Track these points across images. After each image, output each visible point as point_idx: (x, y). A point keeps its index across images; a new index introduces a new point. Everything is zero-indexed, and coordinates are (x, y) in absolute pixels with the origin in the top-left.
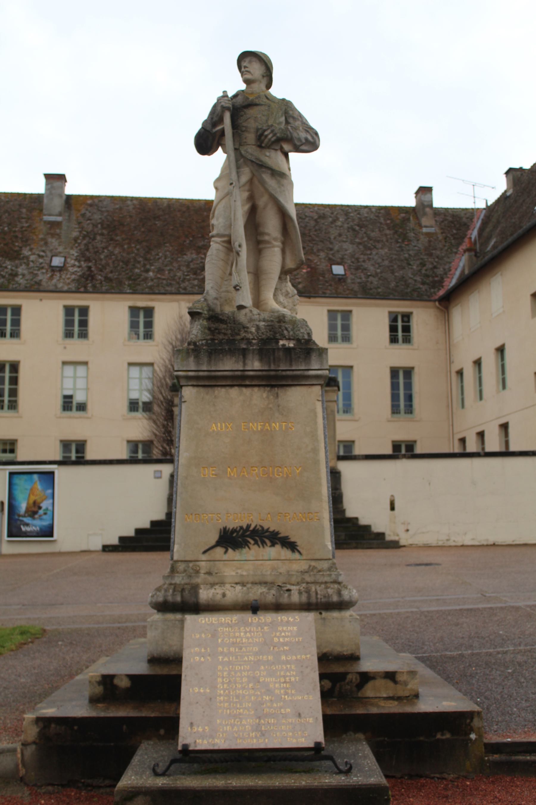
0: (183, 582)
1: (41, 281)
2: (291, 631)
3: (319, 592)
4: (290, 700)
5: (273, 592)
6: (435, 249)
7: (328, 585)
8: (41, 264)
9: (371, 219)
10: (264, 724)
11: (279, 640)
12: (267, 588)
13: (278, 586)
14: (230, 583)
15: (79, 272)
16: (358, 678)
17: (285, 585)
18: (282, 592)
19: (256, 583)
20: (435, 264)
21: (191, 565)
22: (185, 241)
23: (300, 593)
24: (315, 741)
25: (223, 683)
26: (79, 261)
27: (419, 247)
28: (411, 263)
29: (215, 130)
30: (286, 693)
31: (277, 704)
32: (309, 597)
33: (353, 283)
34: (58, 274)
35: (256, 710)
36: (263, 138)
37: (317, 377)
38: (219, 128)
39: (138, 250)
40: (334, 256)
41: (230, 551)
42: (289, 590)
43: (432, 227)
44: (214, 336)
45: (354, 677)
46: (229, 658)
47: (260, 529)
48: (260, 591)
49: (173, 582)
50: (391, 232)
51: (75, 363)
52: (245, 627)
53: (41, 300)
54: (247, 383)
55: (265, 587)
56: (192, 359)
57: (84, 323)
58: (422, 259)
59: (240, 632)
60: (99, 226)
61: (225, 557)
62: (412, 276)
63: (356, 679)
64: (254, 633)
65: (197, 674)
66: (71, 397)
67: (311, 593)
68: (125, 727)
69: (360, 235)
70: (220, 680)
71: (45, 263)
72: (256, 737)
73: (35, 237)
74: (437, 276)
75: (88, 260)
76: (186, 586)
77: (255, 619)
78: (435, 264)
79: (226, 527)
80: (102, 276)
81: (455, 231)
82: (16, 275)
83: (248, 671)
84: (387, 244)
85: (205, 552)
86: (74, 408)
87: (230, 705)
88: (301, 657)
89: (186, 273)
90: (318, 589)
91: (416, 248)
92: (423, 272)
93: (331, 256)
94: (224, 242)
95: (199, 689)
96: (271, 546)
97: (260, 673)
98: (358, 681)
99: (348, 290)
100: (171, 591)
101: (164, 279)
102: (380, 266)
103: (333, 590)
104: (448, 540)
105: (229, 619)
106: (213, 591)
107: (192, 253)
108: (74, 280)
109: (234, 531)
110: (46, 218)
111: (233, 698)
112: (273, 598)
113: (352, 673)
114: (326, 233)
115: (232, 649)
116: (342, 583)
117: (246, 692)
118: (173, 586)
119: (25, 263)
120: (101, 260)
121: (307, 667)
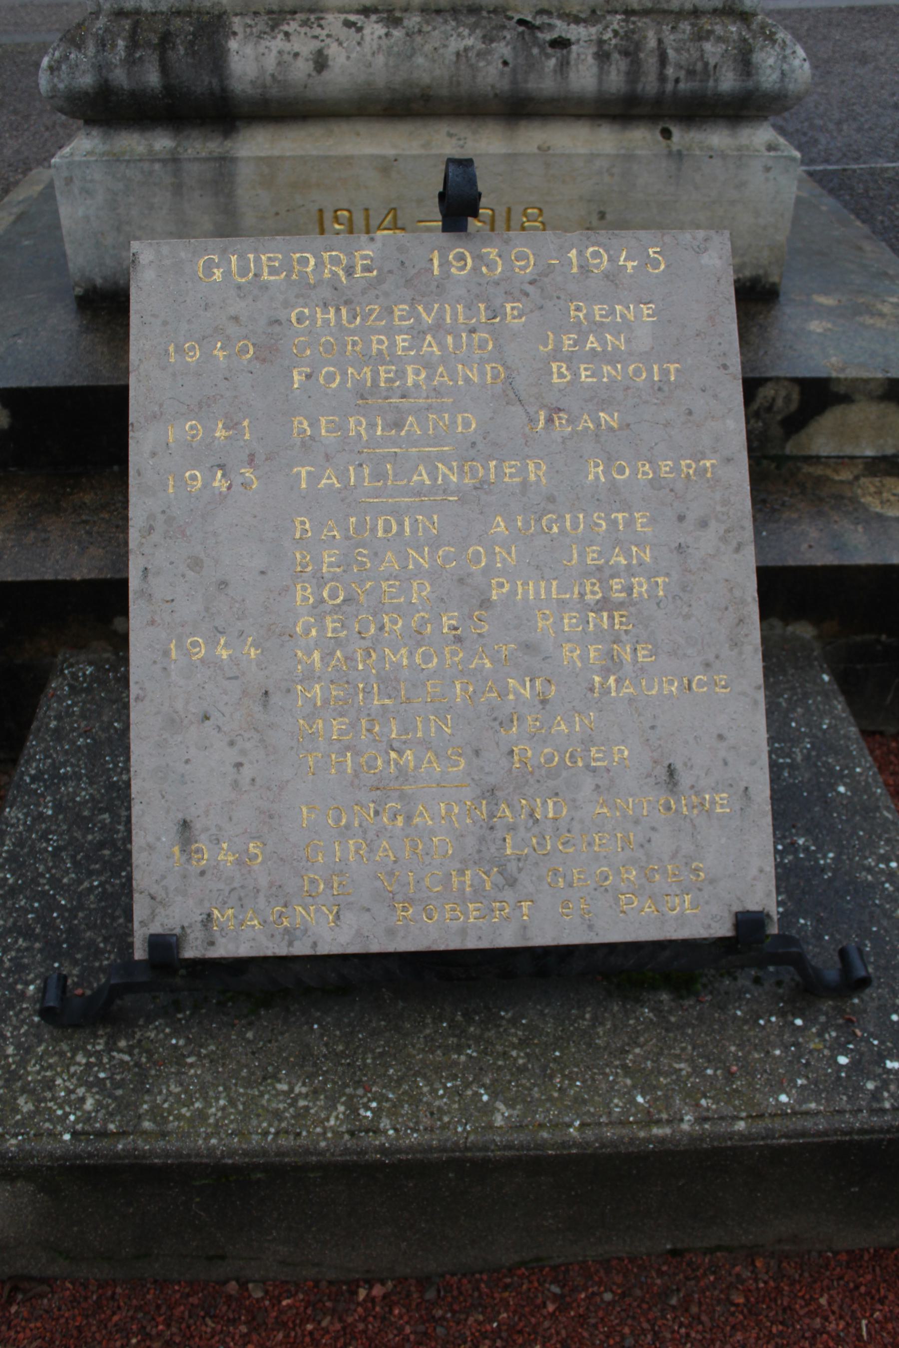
2: (627, 325)
3: (671, 53)
4: (631, 700)
5: (503, 49)
7: (705, 23)
10: (512, 828)
11: (576, 375)
12: (479, 32)
13: (521, 22)
14: (342, 10)
16: (795, 396)
17: (545, 19)
18: (535, 51)
19: (438, 12)
23: (603, 56)
24: (737, 908)
25: (318, 608)
30: (612, 664)
31: (570, 724)
32: (634, 73)
35: (477, 753)
42: (561, 44)
45: (783, 393)
46: (343, 476)
48: (455, 45)
52: (413, 302)
55: (473, 28)
59: (391, 332)
63: (788, 399)
64: (457, 337)
65: (196, 564)
67: (642, 55)
70: (303, 594)
72: (478, 892)
76: (177, 22)
77: (461, 258)
83: (435, 544)
87: (354, 725)
88: (676, 469)
90: (670, 39)
95: (212, 643)
97: (491, 554)
98: (794, 406)
100: (121, 43)
105: (335, 261)
106: (277, 43)
111: (367, 692)
112: (502, 74)
113: (777, 379)
115: (356, 425)
116: (755, 15)
117: (427, 658)
118: (127, 24)
121: (703, 524)
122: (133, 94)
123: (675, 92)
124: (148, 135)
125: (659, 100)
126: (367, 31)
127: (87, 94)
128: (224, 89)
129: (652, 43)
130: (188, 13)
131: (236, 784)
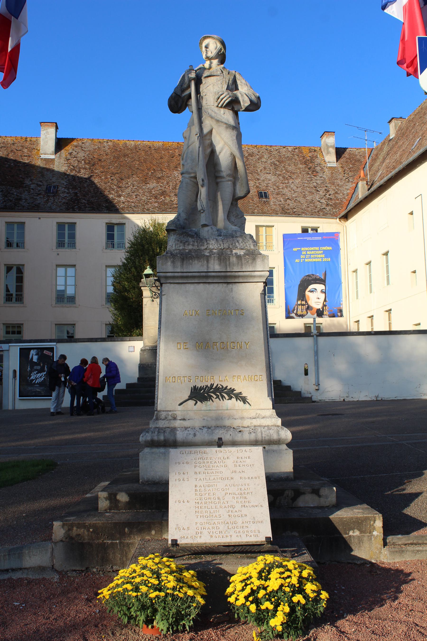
0: (164, 426)
1: (39, 204)
6: (337, 179)
8: (39, 191)
9: (288, 157)
15: (68, 197)
16: (293, 493)
18: (237, 433)
20: (336, 190)
21: (170, 413)
22: (148, 173)
26: (68, 189)
27: (324, 178)
28: (319, 189)
29: (183, 95)
33: (274, 205)
34: (52, 198)
36: (219, 100)
37: (260, 276)
38: (187, 92)
39: (112, 180)
40: (260, 184)
41: (198, 402)
43: (334, 162)
44: (184, 246)
47: (221, 387)
49: (158, 426)
50: (304, 166)
51: (66, 266)
53: (40, 218)
54: (210, 281)
56: (169, 263)
57: (72, 236)
58: (326, 186)
60: (83, 162)
61: (196, 408)
62: (319, 200)
66: (64, 291)
68: (126, 529)
69: (279, 169)
71: (43, 190)
73: (34, 171)
74: (338, 200)
75: (75, 188)
78: (336, 190)
79: (196, 385)
80: (85, 200)
81: (351, 166)
82: (20, 199)
84: (300, 175)
85: (180, 404)
86: (66, 300)
89: (149, 198)
91: (322, 178)
92: (328, 196)
93: (258, 184)
94: (191, 177)
96: (228, 400)
98: (293, 495)
99: (272, 210)
100: (156, 432)
101: (132, 202)
102: (295, 192)
103: (273, 431)
104: (347, 397)
107: (153, 183)
108: (64, 203)
109: (201, 388)
110: (43, 156)
114: (254, 167)
118: (157, 429)
119: (27, 190)
120: (85, 188)
121: (258, 485)
122: (158, 441)
123: (265, 439)
124: (159, 449)
125: (262, 441)
126: (204, 430)
127: (148, 441)
128: (175, 440)
129: (259, 430)
130: (169, 428)
131: (185, 519)
